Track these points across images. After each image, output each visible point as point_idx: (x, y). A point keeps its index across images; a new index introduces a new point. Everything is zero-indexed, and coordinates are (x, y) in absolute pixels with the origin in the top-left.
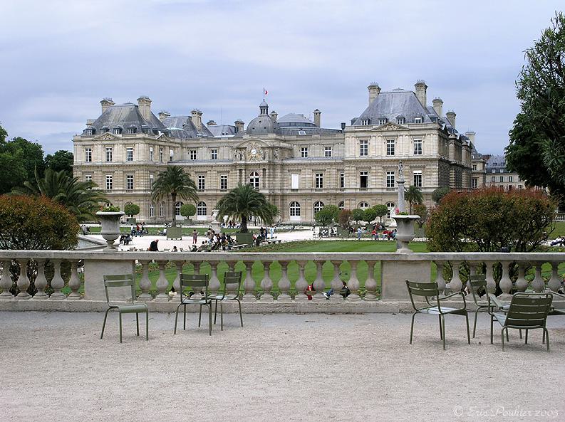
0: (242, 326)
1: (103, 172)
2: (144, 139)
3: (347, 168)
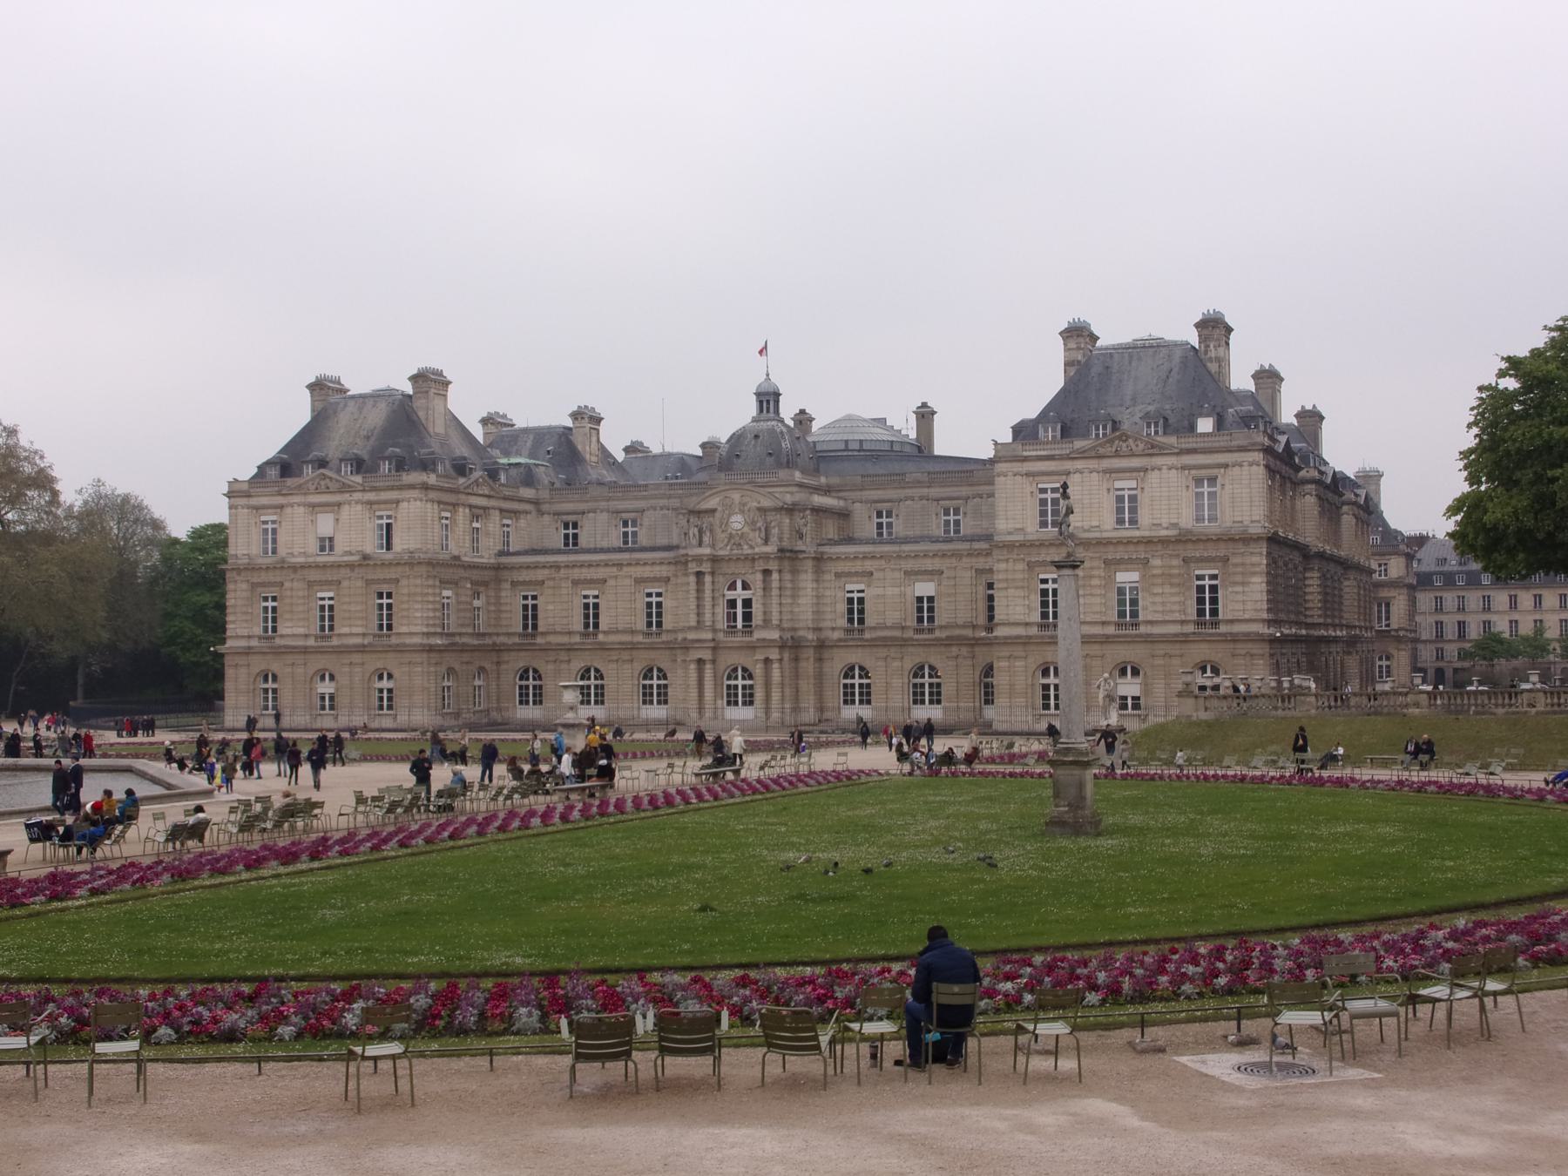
0: (413, 1105)
1: (310, 584)
2: (425, 487)
3: (1003, 566)
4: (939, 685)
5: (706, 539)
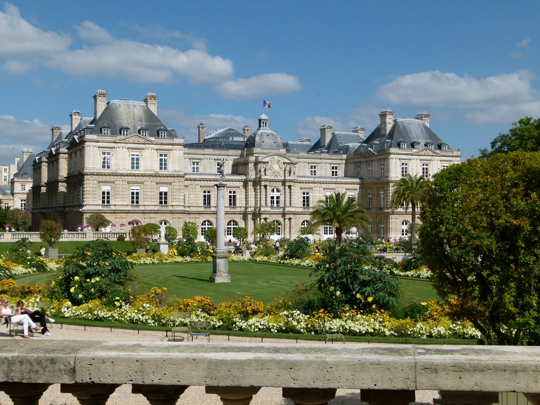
5: (268, 173)
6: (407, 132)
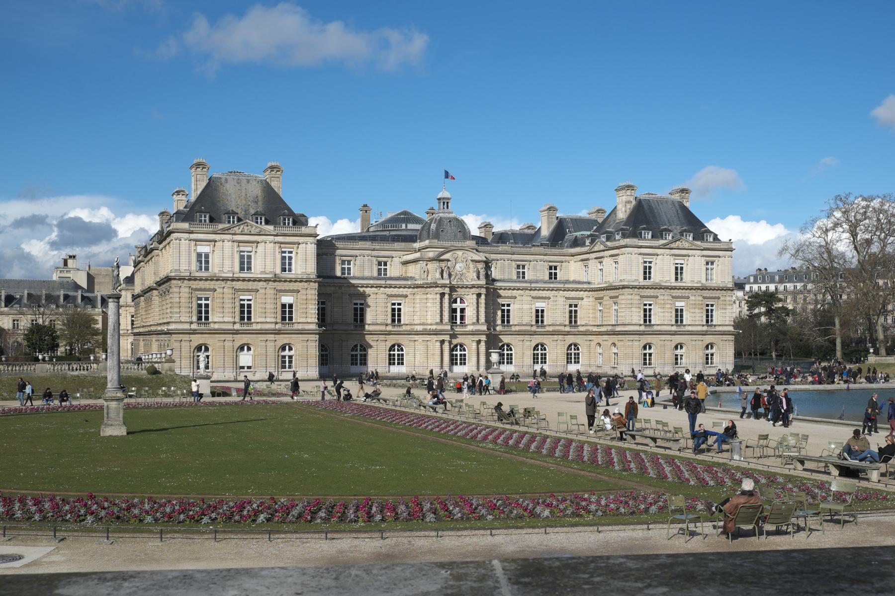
1: (237, 290)
3: (630, 297)
4: (545, 354)
5: (445, 275)
6: (654, 216)
